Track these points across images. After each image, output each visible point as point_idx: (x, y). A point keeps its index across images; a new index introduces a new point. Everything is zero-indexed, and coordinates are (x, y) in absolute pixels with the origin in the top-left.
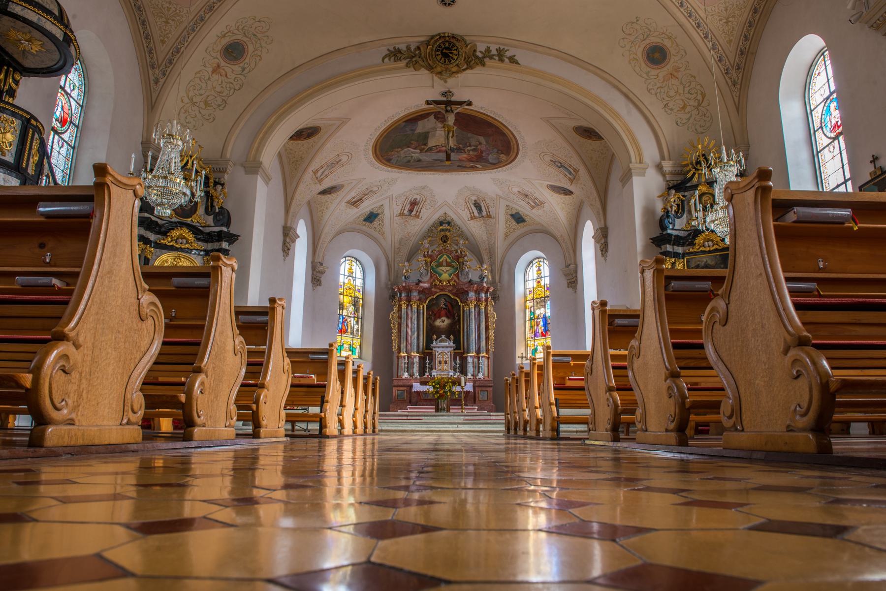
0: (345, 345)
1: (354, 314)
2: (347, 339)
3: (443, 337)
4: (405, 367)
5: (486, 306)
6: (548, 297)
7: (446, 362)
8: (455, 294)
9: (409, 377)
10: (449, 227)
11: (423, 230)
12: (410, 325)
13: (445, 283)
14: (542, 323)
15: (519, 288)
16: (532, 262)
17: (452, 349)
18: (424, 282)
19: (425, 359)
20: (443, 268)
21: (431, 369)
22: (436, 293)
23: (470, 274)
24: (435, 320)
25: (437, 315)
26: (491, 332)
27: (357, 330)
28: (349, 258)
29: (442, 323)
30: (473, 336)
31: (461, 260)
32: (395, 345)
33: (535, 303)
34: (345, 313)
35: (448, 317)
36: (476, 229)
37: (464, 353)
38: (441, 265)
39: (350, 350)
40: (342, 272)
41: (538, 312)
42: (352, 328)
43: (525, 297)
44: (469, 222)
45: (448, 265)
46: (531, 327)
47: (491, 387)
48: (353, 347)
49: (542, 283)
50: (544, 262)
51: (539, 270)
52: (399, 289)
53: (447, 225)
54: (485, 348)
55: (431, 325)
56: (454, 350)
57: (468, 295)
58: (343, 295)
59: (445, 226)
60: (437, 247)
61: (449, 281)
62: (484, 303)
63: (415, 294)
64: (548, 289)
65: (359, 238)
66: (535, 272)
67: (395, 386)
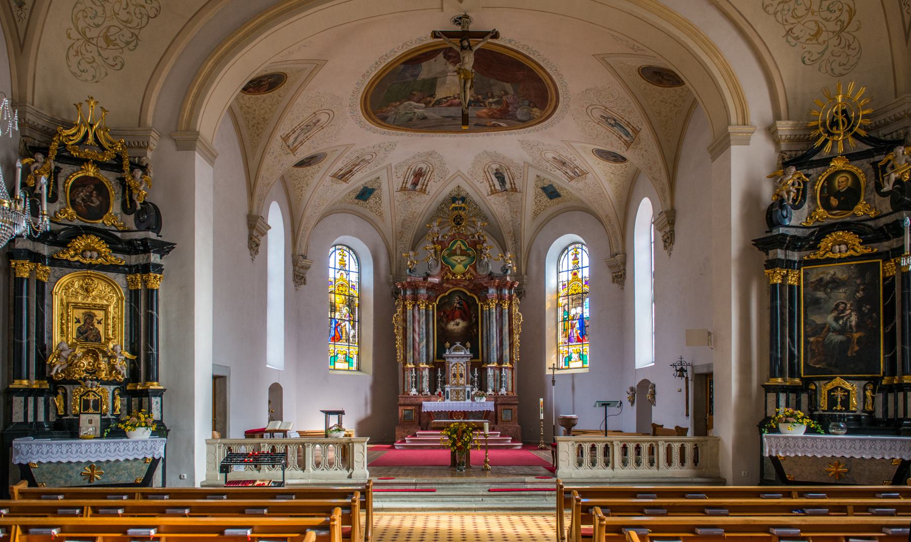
1: (349, 316)
2: (341, 347)
3: (458, 344)
4: (412, 381)
5: (510, 305)
6: (586, 293)
7: (461, 375)
8: (472, 290)
9: (417, 394)
11: (431, 208)
12: (417, 329)
13: (459, 277)
14: (577, 325)
15: (551, 282)
16: (567, 248)
17: (468, 360)
18: (433, 276)
20: (456, 258)
21: (445, 382)
22: (449, 289)
23: (490, 265)
24: (448, 322)
25: (450, 317)
26: (516, 337)
27: (354, 336)
28: (340, 247)
29: (456, 326)
30: (495, 343)
31: (478, 247)
32: (400, 354)
33: (570, 301)
35: (463, 319)
36: (497, 206)
37: (483, 363)
38: (453, 253)
39: (346, 361)
40: (332, 264)
41: (573, 312)
43: (558, 292)
44: (488, 198)
45: (463, 253)
46: (565, 330)
47: (516, 404)
48: (349, 357)
51: (576, 258)
52: (403, 285)
53: (460, 202)
54: (508, 357)
55: (442, 329)
56: (471, 359)
57: (488, 292)
58: (335, 293)
59: (459, 204)
60: (449, 231)
61: (464, 274)
62: (508, 302)
63: (423, 291)
64: (586, 283)
65: (352, 221)
66: (571, 261)
67: (401, 405)
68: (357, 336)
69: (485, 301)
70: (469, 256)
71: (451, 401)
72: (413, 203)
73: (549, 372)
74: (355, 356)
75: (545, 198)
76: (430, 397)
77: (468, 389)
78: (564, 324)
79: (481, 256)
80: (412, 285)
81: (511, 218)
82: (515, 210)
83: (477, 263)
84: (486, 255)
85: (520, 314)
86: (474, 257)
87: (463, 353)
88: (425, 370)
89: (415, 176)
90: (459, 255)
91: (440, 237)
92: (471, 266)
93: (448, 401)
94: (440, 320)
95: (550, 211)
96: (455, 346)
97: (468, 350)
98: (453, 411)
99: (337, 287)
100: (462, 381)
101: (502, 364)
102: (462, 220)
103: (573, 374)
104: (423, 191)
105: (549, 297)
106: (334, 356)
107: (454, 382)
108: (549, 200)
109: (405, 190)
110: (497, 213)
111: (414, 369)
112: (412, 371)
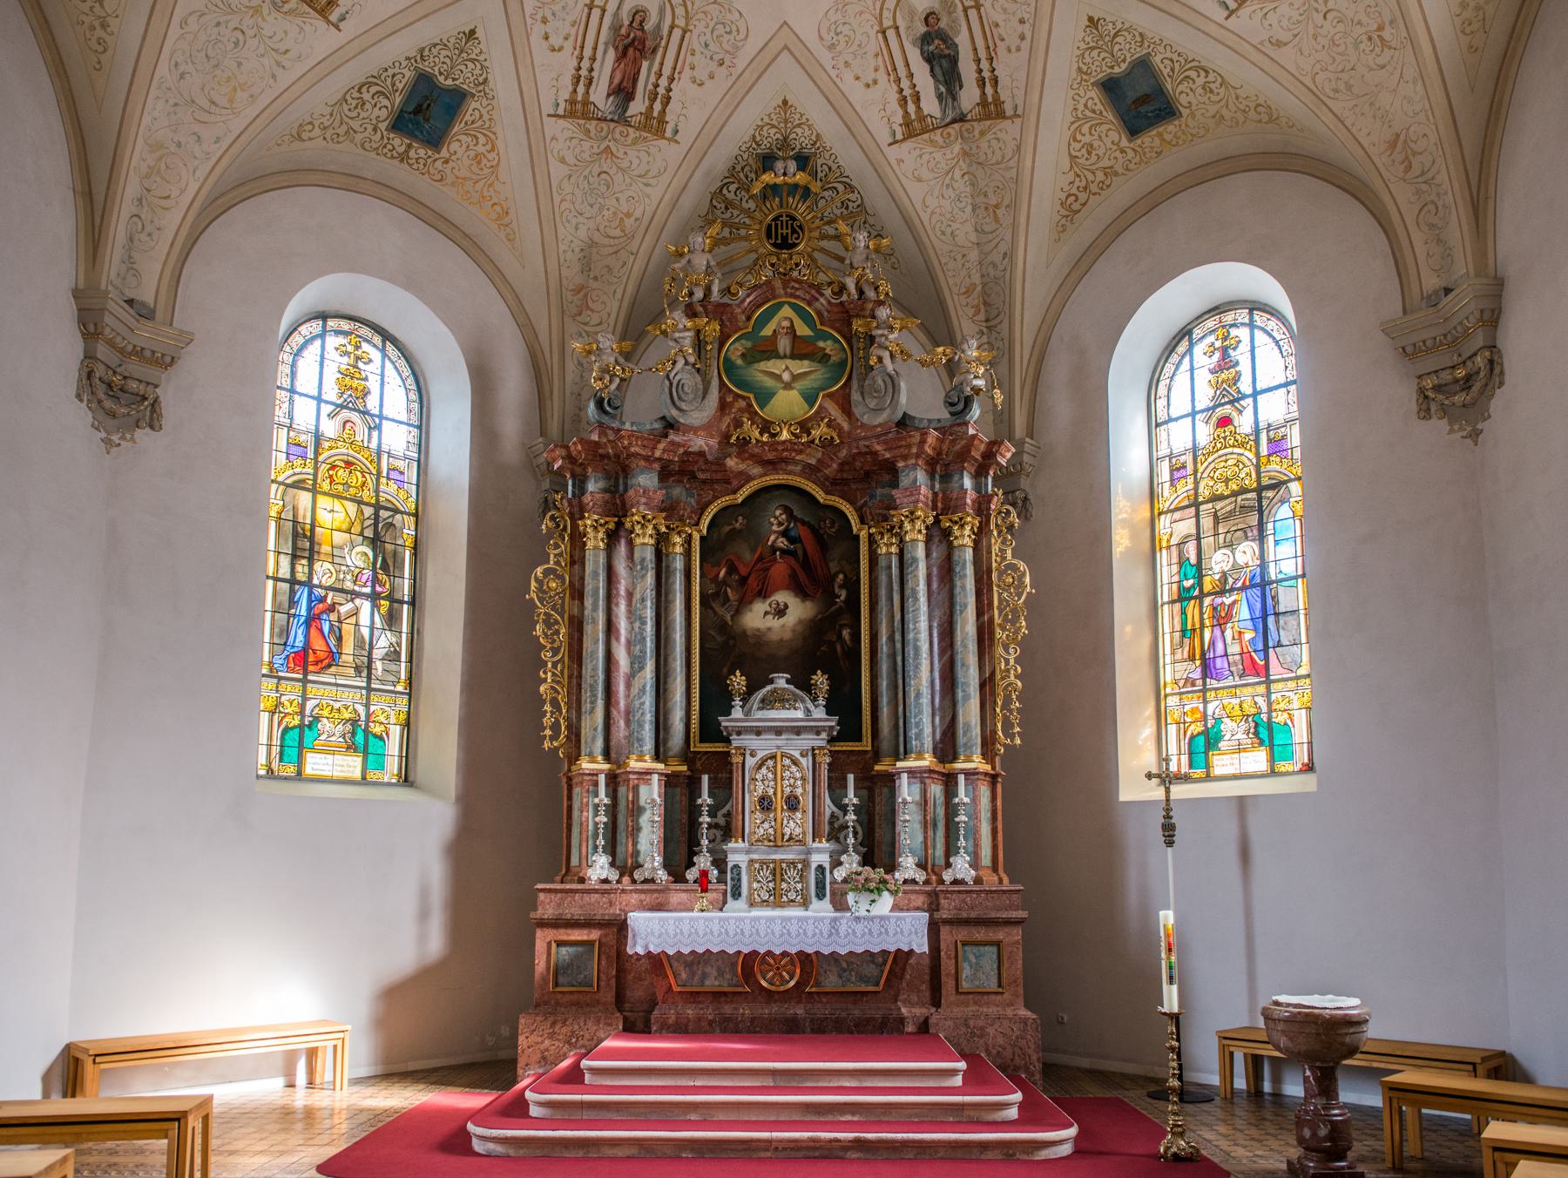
0: (324, 725)
1: (375, 580)
3: (781, 681)
4: (596, 824)
5: (981, 533)
7: (792, 804)
9: (613, 875)
10: (801, 178)
12: (623, 625)
13: (785, 435)
17: (821, 741)
19: (693, 785)
20: (775, 366)
21: (727, 830)
22: (749, 479)
23: (903, 385)
24: (744, 603)
25: (753, 582)
26: (1008, 659)
27: (393, 656)
28: (345, 325)
31: (857, 325)
33: (1207, 523)
34: (323, 573)
35: (802, 593)
37: (876, 756)
38: (766, 351)
39: (351, 748)
41: (1219, 562)
42: (366, 647)
44: (893, 153)
45: (802, 349)
48: (366, 732)
49: (1244, 423)
50: (1251, 325)
51: (1225, 362)
52: (570, 458)
53: (792, 165)
54: (976, 732)
55: (723, 627)
56: (831, 740)
57: (894, 484)
58: (314, 491)
61: (805, 426)
62: (972, 521)
63: (646, 480)
66: (1203, 377)
67: (543, 924)
68: (403, 658)
69: (886, 518)
70: (824, 358)
71: (752, 904)
72: (618, 178)
73: (1135, 787)
74: (395, 731)
75: (1111, 133)
76: (665, 890)
77: (821, 858)
78: (1183, 612)
79: (867, 358)
80: (607, 456)
81: (973, 237)
82: (993, 200)
83: (855, 384)
84: (887, 348)
85: (1022, 566)
86: (842, 364)
87: (800, 714)
88: (648, 782)
89: (622, 55)
90: (785, 357)
91: (715, 289)
92: (830, 396)
93: (737, 909)
94: (716, 595)
95: (1123, 193)
96: (769, 688)
97: (821, 702)
98: (755, 953)
99: (324, 468)
100: (798, 824)
101: (955, 758)
102: (797, 229)
103: (1241, 801)
104: (655, 125)
105: (1126, 510)
106: (301, 727)
107: (766, 829)
108: (1124, 143)
109: (586, 116)
110: (925, 217)
111: (602, 778)
112: (596, 784)
